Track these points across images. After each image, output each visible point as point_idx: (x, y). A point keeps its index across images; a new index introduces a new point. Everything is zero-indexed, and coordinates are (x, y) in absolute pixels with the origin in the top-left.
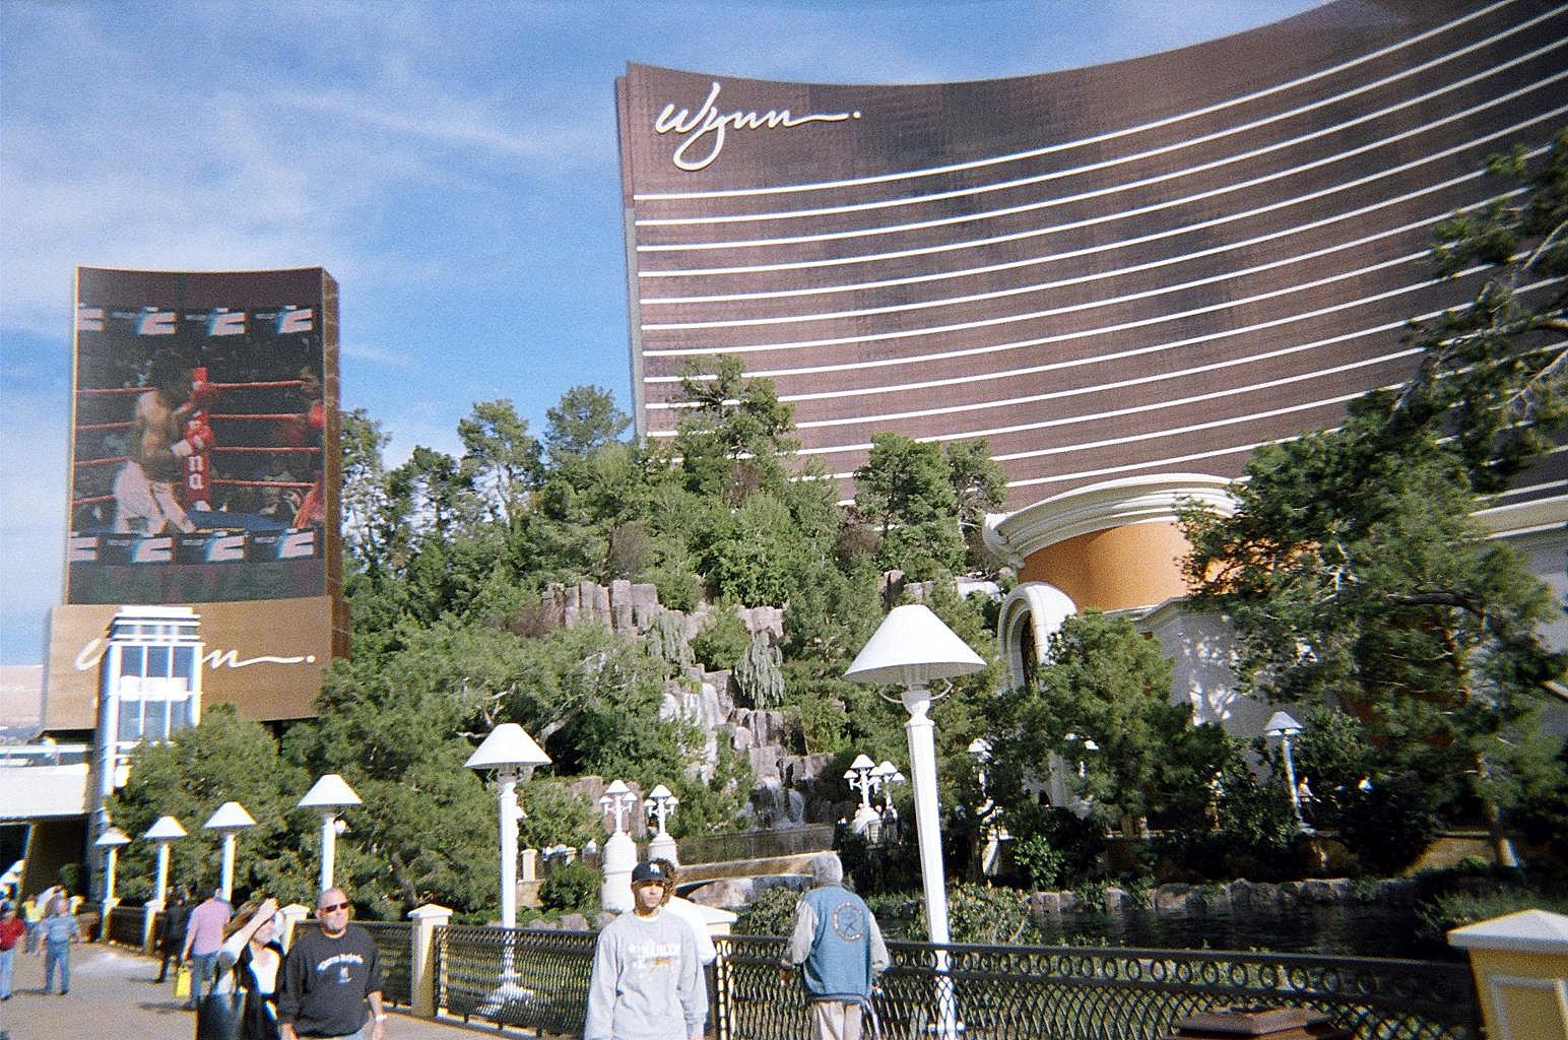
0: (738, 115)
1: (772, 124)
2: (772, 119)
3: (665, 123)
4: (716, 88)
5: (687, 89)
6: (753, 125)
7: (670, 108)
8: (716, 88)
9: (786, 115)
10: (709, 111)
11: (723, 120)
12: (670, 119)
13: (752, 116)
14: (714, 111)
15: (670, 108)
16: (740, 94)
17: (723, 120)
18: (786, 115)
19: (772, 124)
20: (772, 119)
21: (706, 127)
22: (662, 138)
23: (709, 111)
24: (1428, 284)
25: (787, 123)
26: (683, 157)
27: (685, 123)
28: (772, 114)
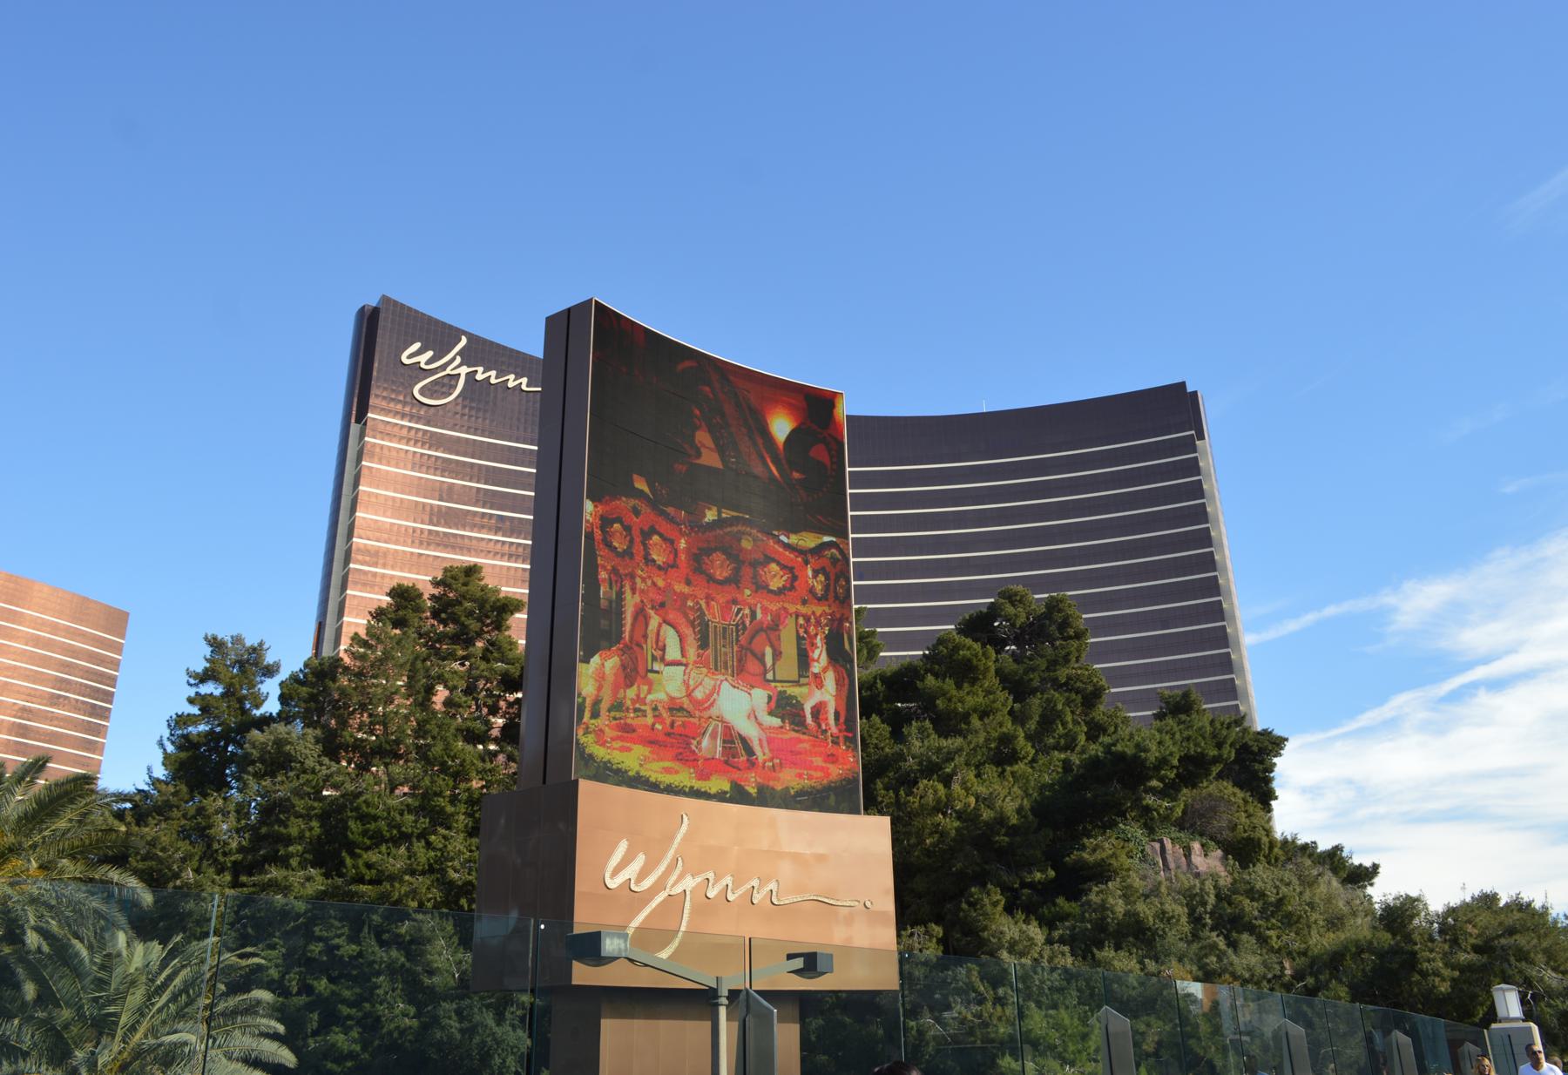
0: (480, 369)
1: (511, 384)
3: (410, 357)
4: (464, 341)
5: (439, 336)
7: (416, 346)
8: (464, 341)
9: (524, 380)
10: (454, 359)
11: (464, 370)
13: (493, 373)
14: (458, 360)
15: (416, 346)
17: (464, 370)
18: (524, 380)
19: (511, 384)
21: (448, 371)
22: (402, 370)
23: (454, 359)
24: (1310, 618)
25: (524, 387)
27: (427, 363)
28: (512, 377)
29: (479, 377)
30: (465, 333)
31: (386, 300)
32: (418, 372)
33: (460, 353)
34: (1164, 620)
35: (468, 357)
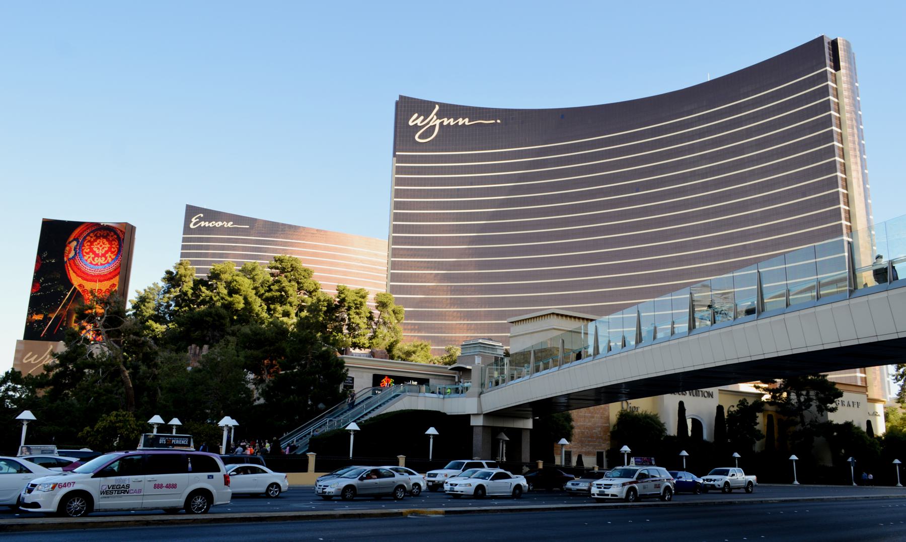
0: (445, 119)
2: (461, 121)
4: (437, 107)
5: (424, 107)
6: (452, 124)
7: (416, 115)
8: (437, 107)
9: (467, 120)
11: (438, 122)
12: (415, 120)
13: (452, 120)
14: (435, 117)
16: (448, 110)
17: (438, 122)
18: (467, 120)
20: (461, 121)
25: (467, 123)
26: (420, 137)
29: (445, 124)
30: (435, 103)
31: (401, 97)
32: (417, 128)
33: (436, 114)
34: (803, 192)
35: (439, 115)
